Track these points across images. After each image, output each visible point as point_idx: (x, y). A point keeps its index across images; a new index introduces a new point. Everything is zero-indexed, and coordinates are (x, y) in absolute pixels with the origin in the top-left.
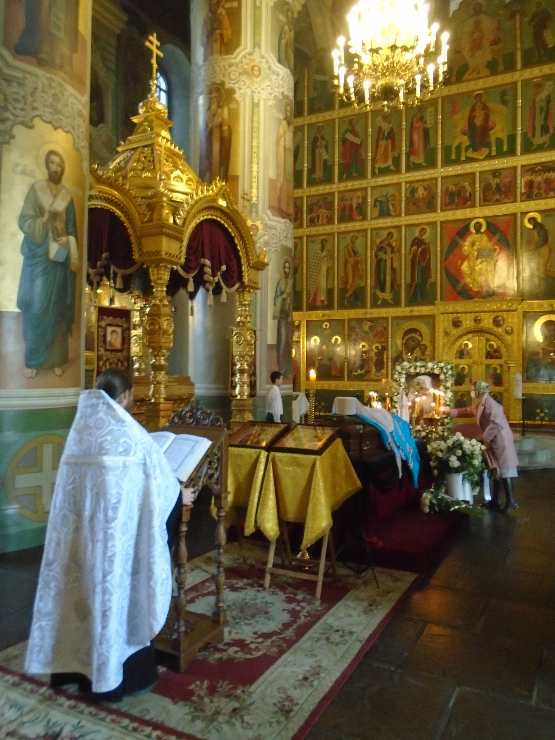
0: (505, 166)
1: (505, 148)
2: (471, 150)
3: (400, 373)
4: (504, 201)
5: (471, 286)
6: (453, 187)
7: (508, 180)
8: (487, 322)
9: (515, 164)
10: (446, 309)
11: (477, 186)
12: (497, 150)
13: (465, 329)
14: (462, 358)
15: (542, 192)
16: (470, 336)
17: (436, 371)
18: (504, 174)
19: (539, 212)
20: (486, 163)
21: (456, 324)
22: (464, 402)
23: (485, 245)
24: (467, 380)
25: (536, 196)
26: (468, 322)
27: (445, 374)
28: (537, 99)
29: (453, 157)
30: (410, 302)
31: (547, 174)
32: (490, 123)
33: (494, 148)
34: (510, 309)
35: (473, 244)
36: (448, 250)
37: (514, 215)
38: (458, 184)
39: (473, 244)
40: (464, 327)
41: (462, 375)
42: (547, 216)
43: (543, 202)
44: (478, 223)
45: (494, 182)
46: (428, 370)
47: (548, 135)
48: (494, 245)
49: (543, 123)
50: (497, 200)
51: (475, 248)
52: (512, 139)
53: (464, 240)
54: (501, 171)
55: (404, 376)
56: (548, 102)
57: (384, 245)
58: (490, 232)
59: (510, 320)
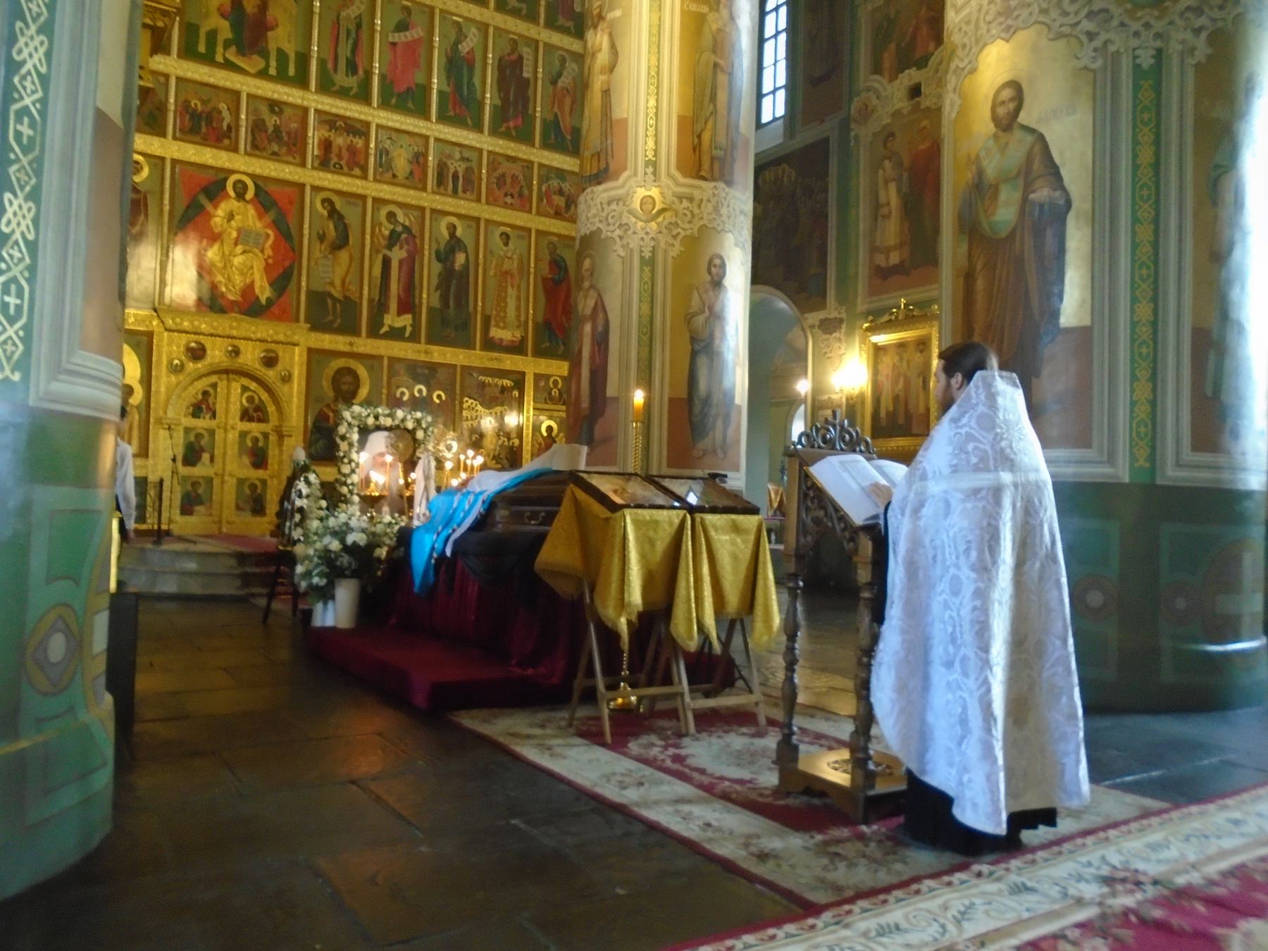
0: (291, 100)
1: (292, 71)
2: (233, 49)
3: (349, 424)
4: (286, 159)
5: (224, 289)
6: (199, 103)
7: (294, 125)
8: (251, 356)
9: (305, 103)
10: (176, 324)
11: (243, 117)
12: (277, 69)
13: (211, 365)
14: (199, 417)
15: (343, 163)
16: (214, 379)
17: (410, 425)
18: (288, 112)
19: (340, 193)
20: (257, 82)
21: (197, 353)
22: (198, 496)
23: (251, 224)
24: (206, 456)
25: (334, 166)
26: (216, 353)
27: (425, 430)
28: (343, 14)
29: (202, 48)
31: (351, 137)
32: (268, 17)
33: (273, 63)
34: (289, 340)
35: (231, 216)
36: (183, 216)
37: (302, 186)
38: (210, 100)
39: (231, 216)
40: (208, 360)
41: (197, 448)
42: (349, 203)
43: (345, 179)
44: (239, 181)
45: (271, 121)
46: (397, 422)
48: (266, 227)
49: (349, 55)
50: (274, 154)
51: (233, 223)
52: (303, 59)
53: (216, 207)
54: (283, 107)
55: (356, 429)
56: (359, 26)
58: (261, 204)
59: (287, 360)
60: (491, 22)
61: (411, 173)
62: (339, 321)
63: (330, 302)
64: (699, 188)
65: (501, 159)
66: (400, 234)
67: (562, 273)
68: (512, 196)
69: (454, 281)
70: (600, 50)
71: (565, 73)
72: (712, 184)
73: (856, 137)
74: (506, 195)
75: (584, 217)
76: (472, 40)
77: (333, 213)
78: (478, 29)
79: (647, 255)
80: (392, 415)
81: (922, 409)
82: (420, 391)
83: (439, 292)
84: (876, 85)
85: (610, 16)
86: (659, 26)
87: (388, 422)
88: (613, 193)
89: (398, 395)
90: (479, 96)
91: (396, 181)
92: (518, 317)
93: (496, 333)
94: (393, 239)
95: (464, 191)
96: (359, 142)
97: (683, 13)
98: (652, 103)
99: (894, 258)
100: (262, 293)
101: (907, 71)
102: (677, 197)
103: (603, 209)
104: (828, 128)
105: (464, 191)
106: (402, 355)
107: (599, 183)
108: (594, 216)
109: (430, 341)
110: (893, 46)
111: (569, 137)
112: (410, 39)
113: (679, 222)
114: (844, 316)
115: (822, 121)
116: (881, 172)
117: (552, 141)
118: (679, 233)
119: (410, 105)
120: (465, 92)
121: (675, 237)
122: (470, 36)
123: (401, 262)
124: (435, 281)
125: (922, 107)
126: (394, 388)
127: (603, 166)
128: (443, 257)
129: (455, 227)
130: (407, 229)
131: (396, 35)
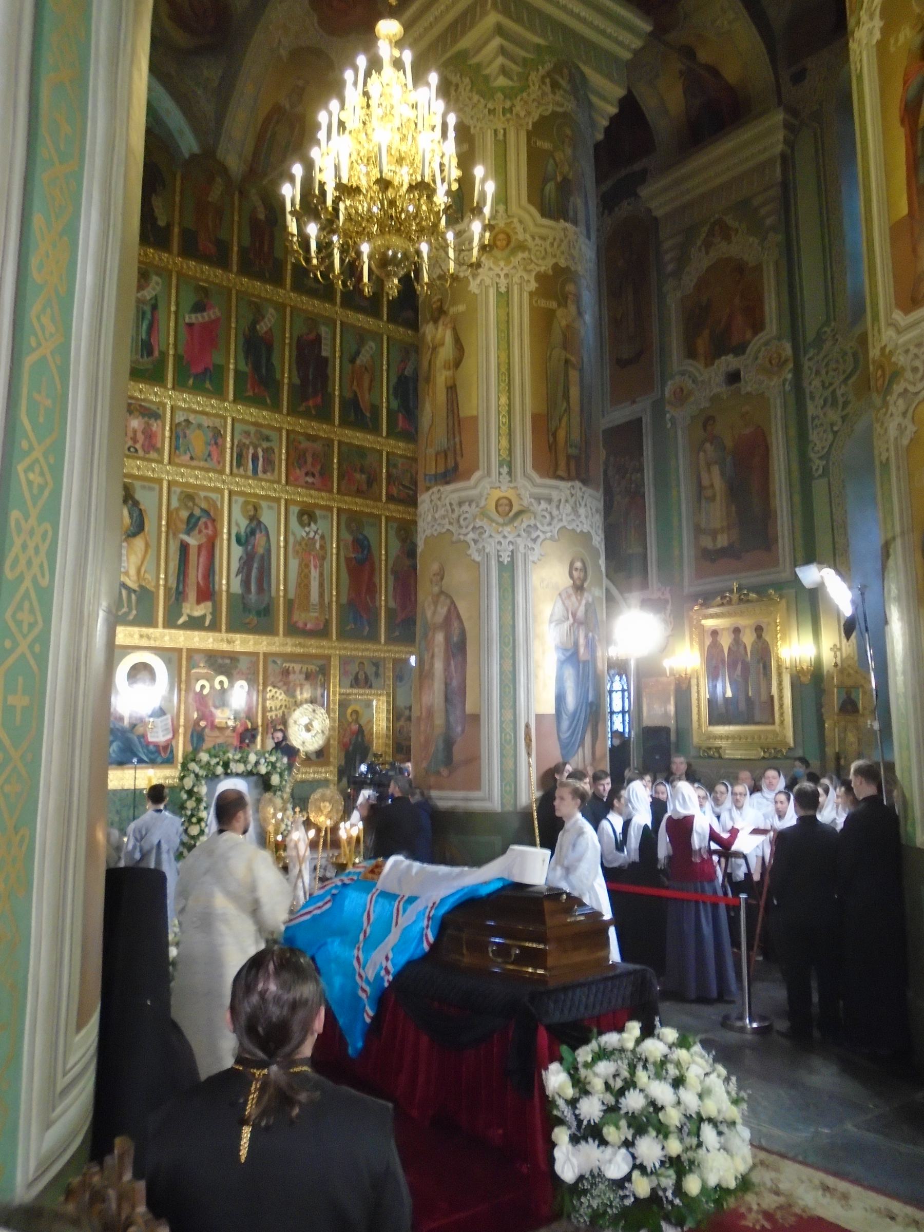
3: (197, 776)
15: (138, 446)
17: (263, 770)
27: (281, 775)
42: (143, 487)
46: (249, 767)
47: (150, 359)
49: (144, 337)
60: (287, 301)
61: (209, 455)
62: (134, 612)
63: (124, 592)
64: (557, 488)
65: (301, 438)
66: (199, 519)
67: (365, 552)
68: (313, 475)
69: (255, 565)
70: (443, 344)
71: (363, 351)
72: (570, 484)
73: (673, 420)
74: (307, 474)
75: (430, 518)
76: (270, 320)
77: (129, 497)
78: (275, 309)
79: (506, 560)
80: (244, 760)
81: (764, 697)
82: (221, 683)
83: (240, 577)
84: (692, 369)
85: (453, 310)
86: (508, 322)
87: (240, 768)
88: (463, 494)
89: (198, 689)
90: (278, 376)
91: (194, 463)
93: (299, 617)
94: (192, 524)
95: (265, 472)
96: (155, 426)
97: (532, 309)
98: (504, 400)
99: (722, 541)
101: (723, 358)
102: (535, 499)
103: (453, 511)
104: (641, 408)
105: (265, 472)
106: (203, 646)
107: (448, 483)
108: (444, 517)
109: (231, 629)
110: (706, 333)
111: (368, 415)
112: (207, 319)
113: (539, 525)
114: (668, 596)
115: (634, 402)
116: (701, 454)
117: (352, 418)
118: (538, 537)
119: (208, 385)
120: (264, 371)
121: (535, 540)
122: (268, 315)
123: (200, 547)
124: (235, 566)
125: (743, 392)
126: (193, 681)
127: (451, 464)
128: (243, 540)
129: (255, 509)
130: (206, 512)
131: (193, 316)
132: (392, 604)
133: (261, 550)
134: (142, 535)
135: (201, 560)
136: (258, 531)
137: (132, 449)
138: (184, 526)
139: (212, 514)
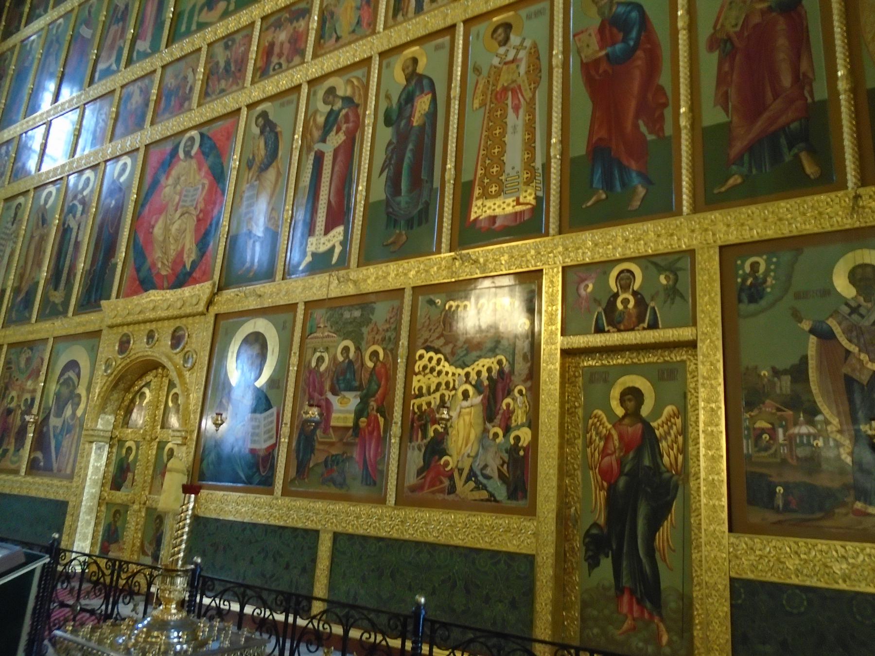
4: (230, 90)
24: (130, 475)
25: (274, 69)
30: (82, 306)
41: (125, 466)
50: (223, 91)
51: (179, 188)
53: (167, 178)
57: (76, 202)
67: (634, 34)
69: (410, 146)
89: (313, 364)
91: (338, 45)
92: (529, 164)
100: (189, 257)
123: (336, 152)
128: (394, 117)
129: (415, 61)
130: (348, 101)
132: (713, 116)
133: (416, 121)
134: (274, 164)
135: (337, 168)
136: (418, 93)
137: (277, 67)
138: (320, 132)
139: (356, 100)
